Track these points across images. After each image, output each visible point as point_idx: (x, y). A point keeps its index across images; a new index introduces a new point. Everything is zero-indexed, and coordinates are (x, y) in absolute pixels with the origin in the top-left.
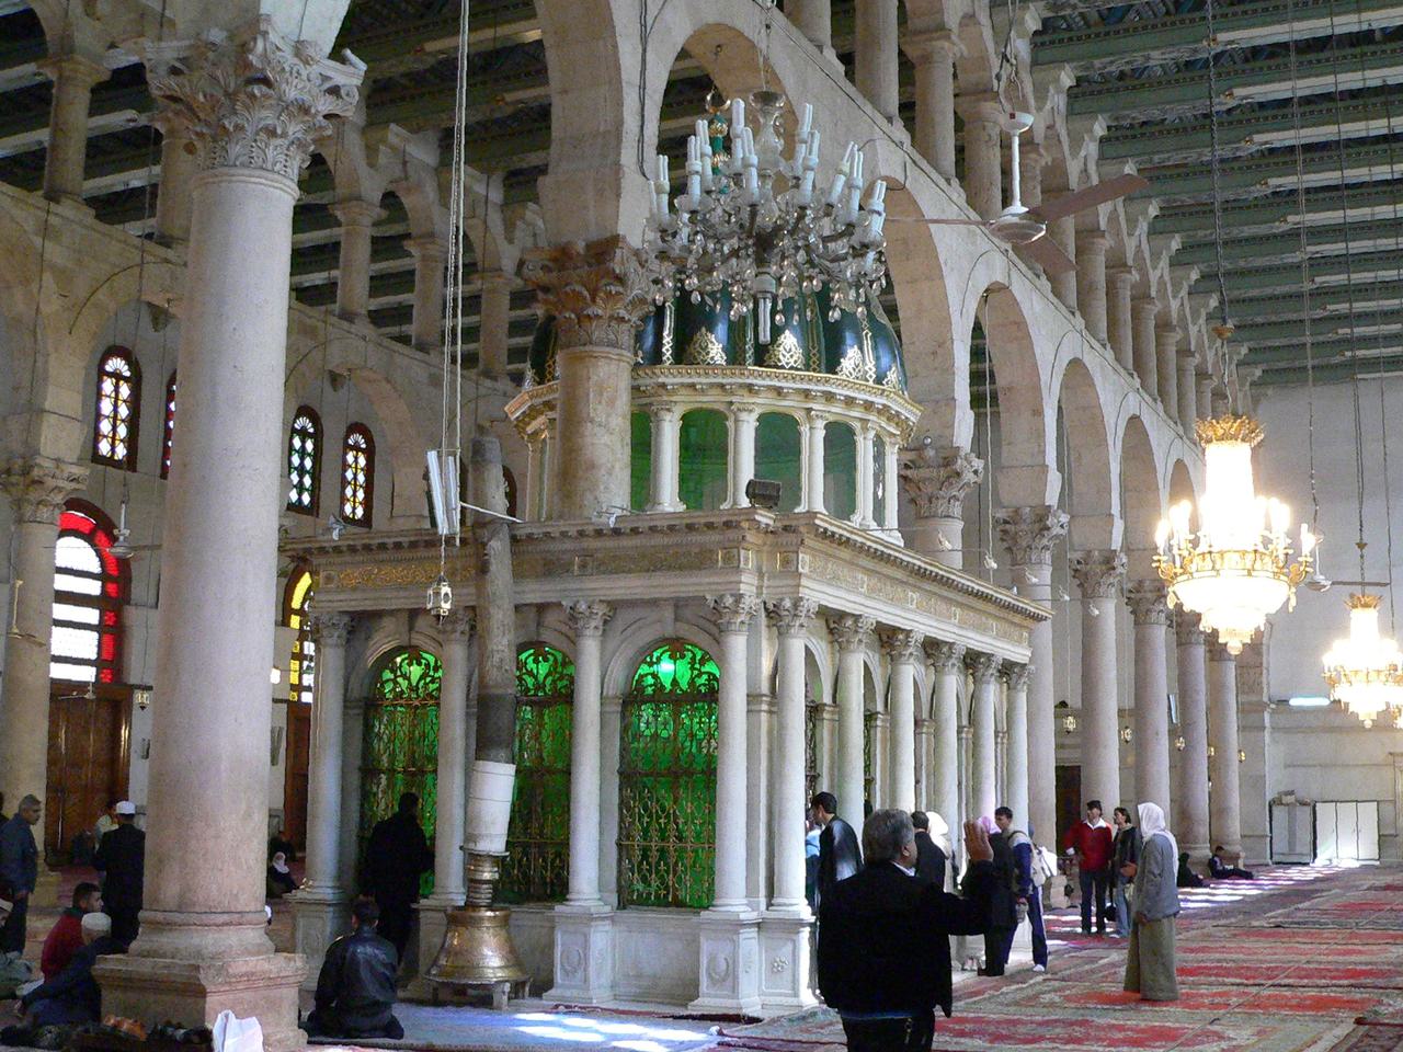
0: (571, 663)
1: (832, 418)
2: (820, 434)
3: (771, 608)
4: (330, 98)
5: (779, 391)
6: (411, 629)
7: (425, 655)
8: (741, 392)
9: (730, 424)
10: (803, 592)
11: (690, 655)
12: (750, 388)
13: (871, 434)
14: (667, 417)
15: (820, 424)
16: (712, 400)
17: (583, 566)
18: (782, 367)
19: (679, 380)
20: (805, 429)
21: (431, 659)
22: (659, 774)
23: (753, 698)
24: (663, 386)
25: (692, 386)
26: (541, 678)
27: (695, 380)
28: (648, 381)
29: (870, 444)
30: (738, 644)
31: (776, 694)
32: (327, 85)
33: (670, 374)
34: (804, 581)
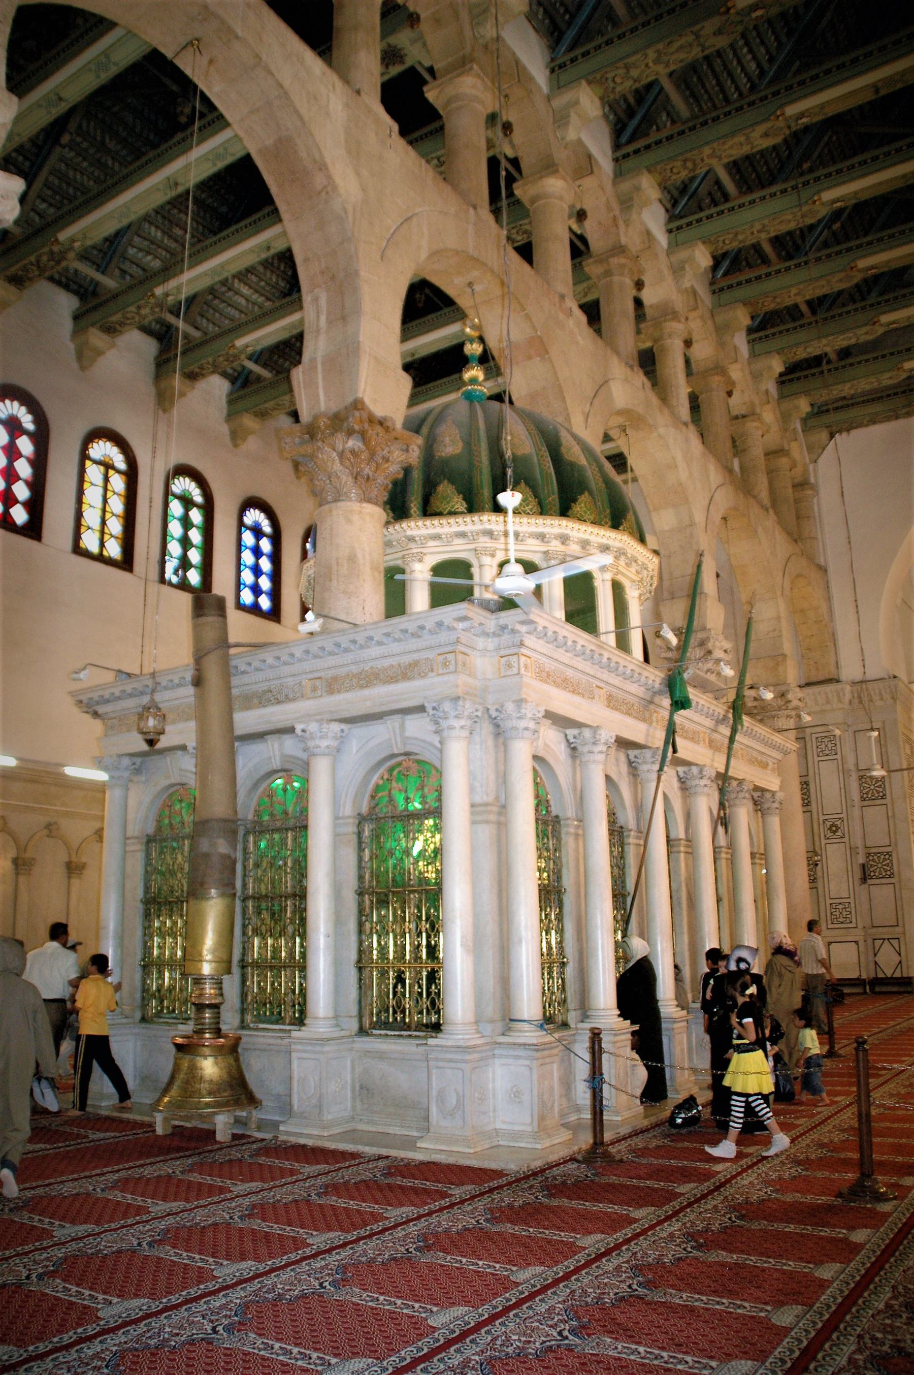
3: (494, 714)
12: (490, 533)
14: (417, 566)
16: (458, 550)
19: (424, 532)
24: (411, 539)
28: (397, 536)
29: (609, 586)
33: (417, 527)
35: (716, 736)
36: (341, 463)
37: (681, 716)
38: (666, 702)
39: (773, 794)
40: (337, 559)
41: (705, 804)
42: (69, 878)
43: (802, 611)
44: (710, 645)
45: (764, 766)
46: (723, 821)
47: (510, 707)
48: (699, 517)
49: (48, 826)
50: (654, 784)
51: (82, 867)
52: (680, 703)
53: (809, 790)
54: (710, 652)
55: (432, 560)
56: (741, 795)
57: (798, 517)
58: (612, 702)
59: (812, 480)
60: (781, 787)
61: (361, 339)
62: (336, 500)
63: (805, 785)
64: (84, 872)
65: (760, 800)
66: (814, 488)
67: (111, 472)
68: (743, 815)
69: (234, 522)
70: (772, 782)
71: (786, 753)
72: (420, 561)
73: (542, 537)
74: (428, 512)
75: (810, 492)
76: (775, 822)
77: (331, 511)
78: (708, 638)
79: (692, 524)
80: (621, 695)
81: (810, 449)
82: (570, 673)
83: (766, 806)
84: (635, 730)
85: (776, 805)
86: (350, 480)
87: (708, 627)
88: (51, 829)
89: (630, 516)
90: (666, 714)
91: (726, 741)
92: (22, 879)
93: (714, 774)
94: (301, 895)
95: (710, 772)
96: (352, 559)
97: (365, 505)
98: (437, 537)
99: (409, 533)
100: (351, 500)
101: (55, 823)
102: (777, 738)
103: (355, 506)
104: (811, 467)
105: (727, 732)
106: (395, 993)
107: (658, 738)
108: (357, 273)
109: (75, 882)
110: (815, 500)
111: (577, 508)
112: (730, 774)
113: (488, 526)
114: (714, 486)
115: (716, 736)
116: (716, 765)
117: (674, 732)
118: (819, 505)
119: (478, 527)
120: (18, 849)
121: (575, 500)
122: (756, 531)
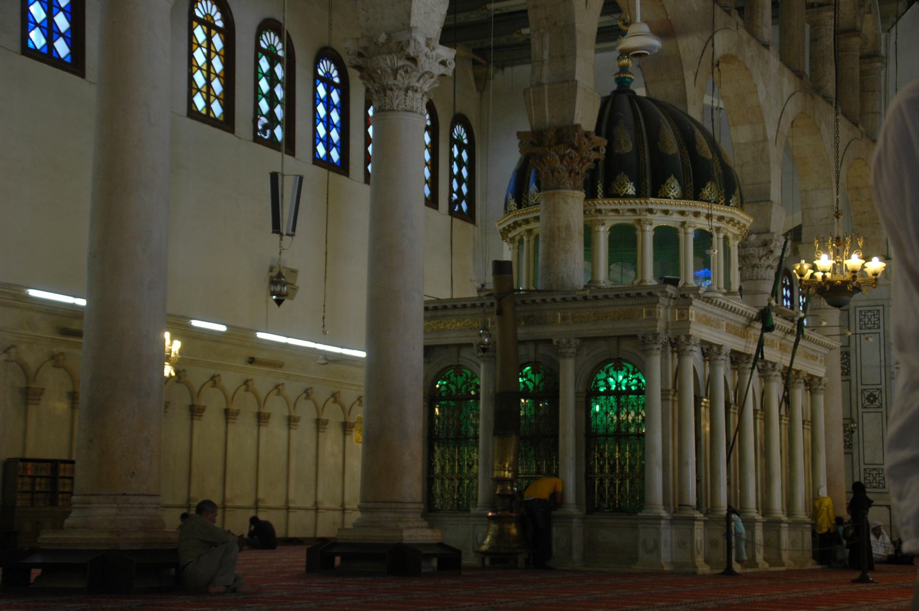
0: (476, 377)
1: (699, 226)
2: (691, 237)
3: (673, 341)
4: (442, 67)
5: (666, 212)
6: (458, 356)
7: (625, 364)
8: (644, 213)
9: (639, 233)
10: (692, 332)
11: (625, 369)
12: (651, 211)
13: (721, 236)
14: (602, 229)
15: (691, 230)
16: (629, 219)
17: (564, 318)
18: (669, 198)
19: (608, 207)
20: (682, 235)
21: (469, 373)
22: (610, 436)
23: (665, 393)
24: (599, 211)
25: (617, 211)
26: (537, 383)
27: (618, 207)
30: (656, 362)
31: (678, 389)
32: (439, 60)
33: (603, 204)
34: (692, 325)
35: (784, 342)
36: (561, 163)
37: (766, 335)
38: (759, 326)
39: (820, 379)
40: (559, 228)
41: (776, 389)
42: (192, 419)
43: (857, 188)
44: (772, 246)
45: (815, 358)
46: (787, 400)
47: (683, 338)
48: (771, 133)
49: (213, 378)
50: (749, 376)
51: (202, 410)
52: (768, 327)
53: (849, 361)
54: (772, 252)
55: (609, 224)
56: (798, 381)
57: (863, 90)
58: (731, 330)
59: (883, 52)
60: (826, 374)
61: (577, 77)
62: (558, 188)
63: (845, 355)
64: (204, 414)
65: (811, 383)
66: (884, 60)
67: (213, 32)
68: (800, 395)
69: (310, 76)
70: (819, 371)
71: (831, 348)
72: (603, 224)
73: (682, 213)
74: (609, 194)
75: (879, 65)
76: (821, 399)
77: (554, 195)
78: (771, 241)
79: (765, 140)
80: (733, 323)
81: (884, 18)
82: (709, 315)
83: (814, 387)
84: (739, 344)
85: (822, 387)
86: (567, 174)
87: (772, 230)
88: (214, 380)
89: (737, 191)
90: (759, 333)
91: (792, 345)
92: (196, 422)
93: (782, 368)
94: (556, 436)
95: (779, 367)
96: (568, 228)
97: (576, 192)
98: (617, 211)
99: (598, 207)
100: (566, 188)
101: (184, 370)
102: (826, 341)
103: (570, 192)
104: (883, 36)
105: (793, 339)
106: (609, 492)
107: (752, 349)
108: (574, 25)
109: (196, 423)
110: (883, 73)
111: (706, 192)
112: (793, 367)
113: (650, 206)
114: (786, 98)
115: (784, 342)
116: (783, 361)
117: (762, 345)
118: (886, 75)
119: (644, 207)
120: (192, 398)
121: (704, 186)
122: (819, 130)
